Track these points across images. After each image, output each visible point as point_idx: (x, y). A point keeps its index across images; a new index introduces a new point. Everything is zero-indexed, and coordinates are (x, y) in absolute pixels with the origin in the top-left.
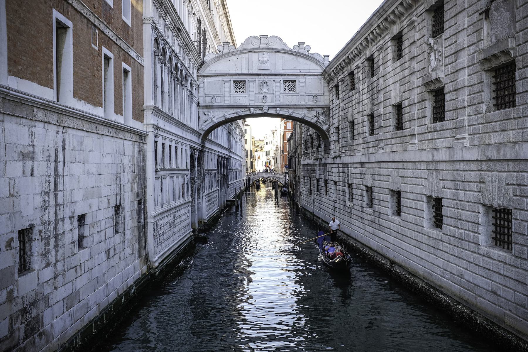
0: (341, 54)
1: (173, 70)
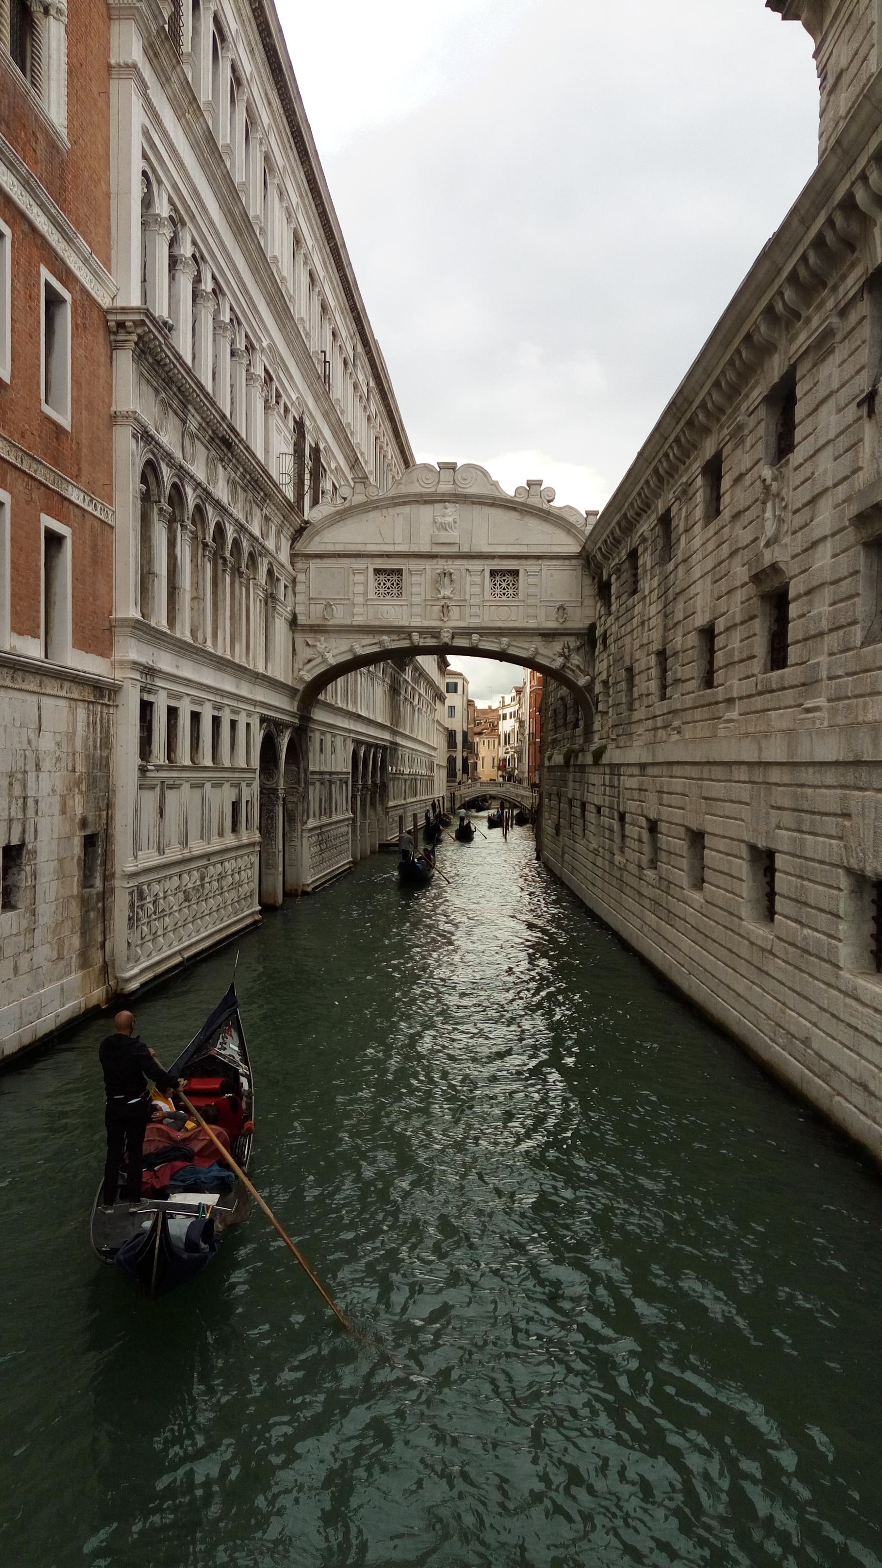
1: (209, 539)
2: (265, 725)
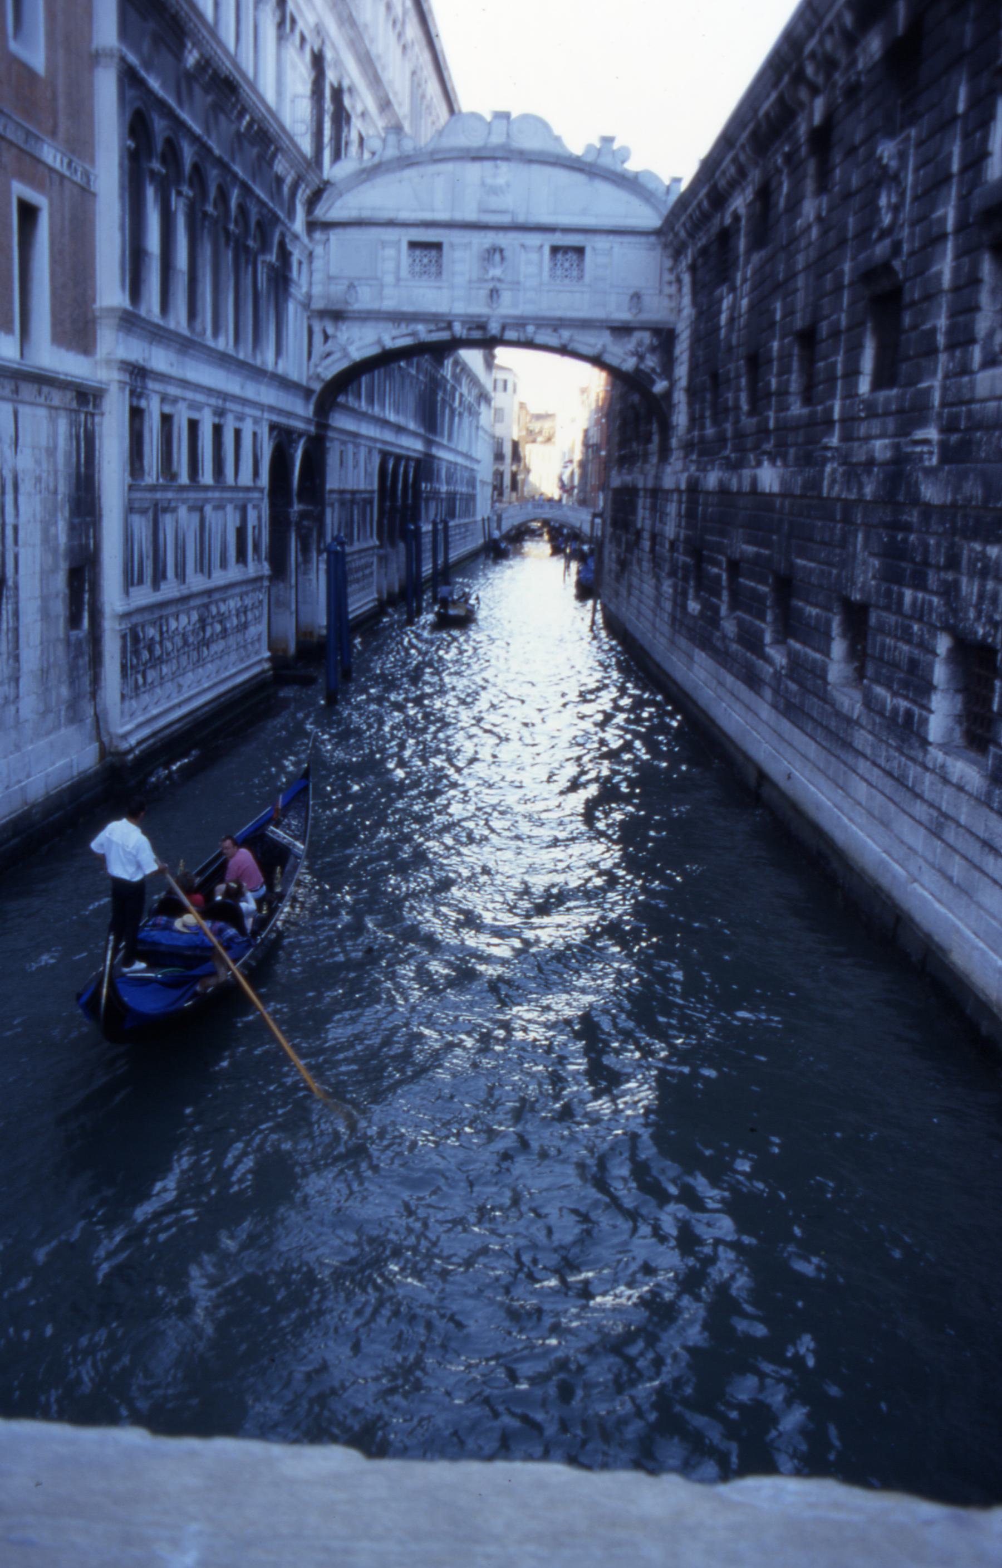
2: (275, 433)
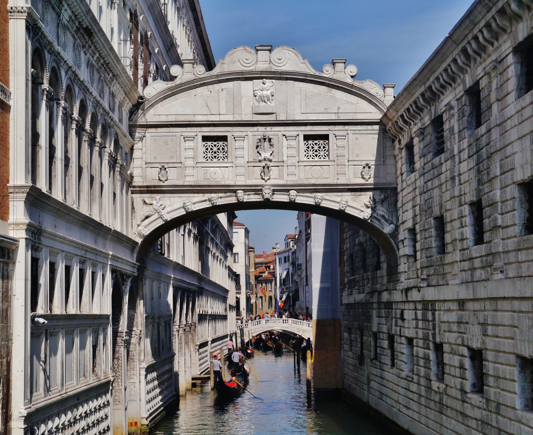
0: (417, 82)
